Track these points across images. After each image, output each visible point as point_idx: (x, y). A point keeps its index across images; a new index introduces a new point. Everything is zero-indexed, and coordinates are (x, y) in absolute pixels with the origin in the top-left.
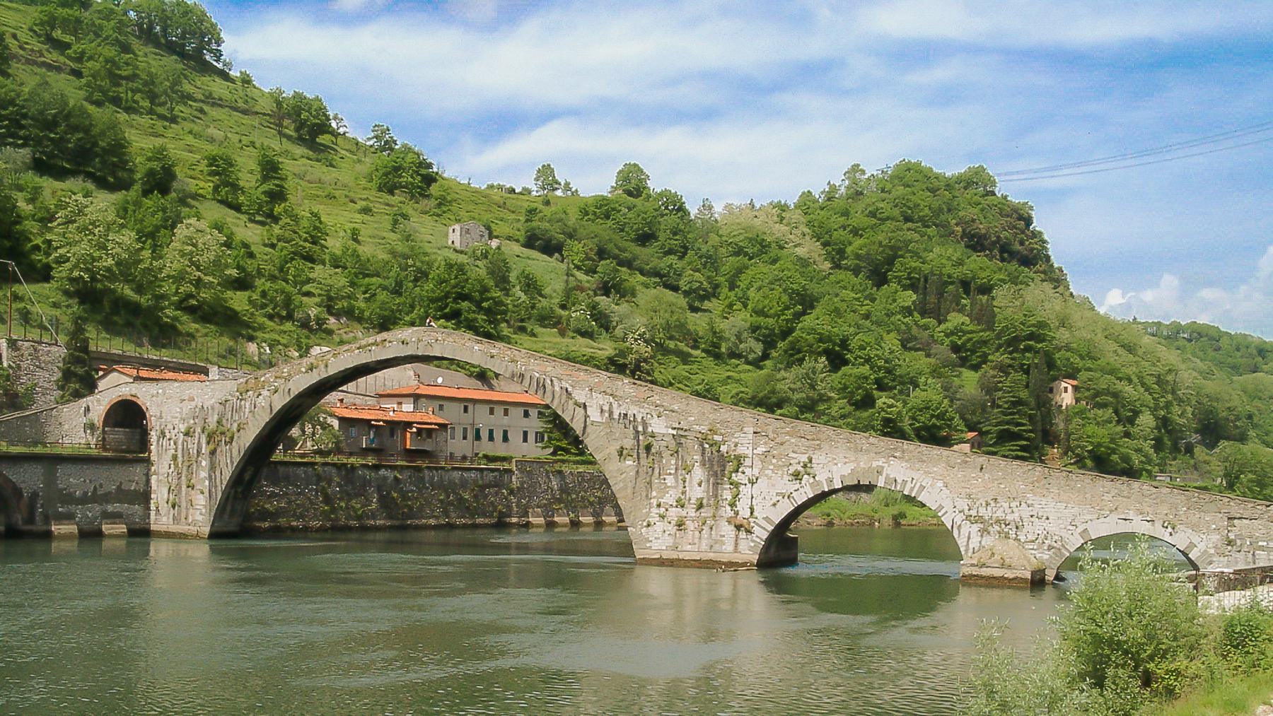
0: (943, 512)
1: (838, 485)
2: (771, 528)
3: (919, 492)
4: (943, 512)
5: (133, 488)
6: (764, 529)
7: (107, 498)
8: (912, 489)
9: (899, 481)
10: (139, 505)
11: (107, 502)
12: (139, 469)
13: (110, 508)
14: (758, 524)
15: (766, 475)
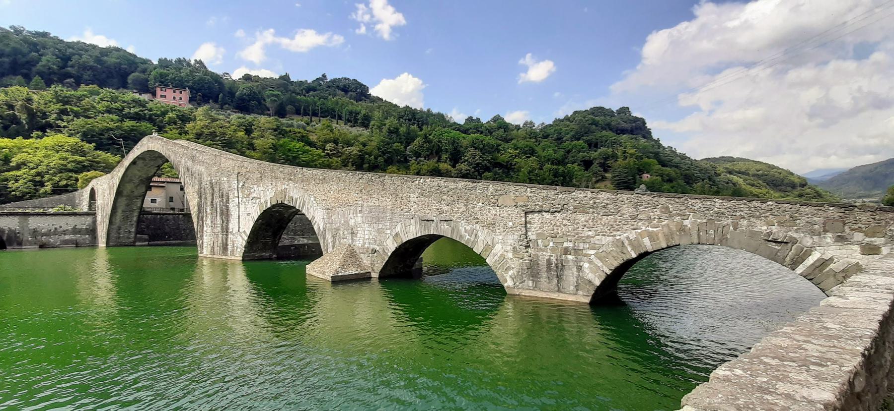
0: (314, 222)
1: (269, 206)
2: (246, 238)
3: (303, 207)
4: (314, 222)
5: (84, 227)
6: (243, 239)
7: (65, 232)
8: (300, 205)
9: (294, 199)
10: (89, 235)
11: (65, 235)
12: (89, 219)
13: (67, 237)
14: (241, 236)
15: (244, 202)
